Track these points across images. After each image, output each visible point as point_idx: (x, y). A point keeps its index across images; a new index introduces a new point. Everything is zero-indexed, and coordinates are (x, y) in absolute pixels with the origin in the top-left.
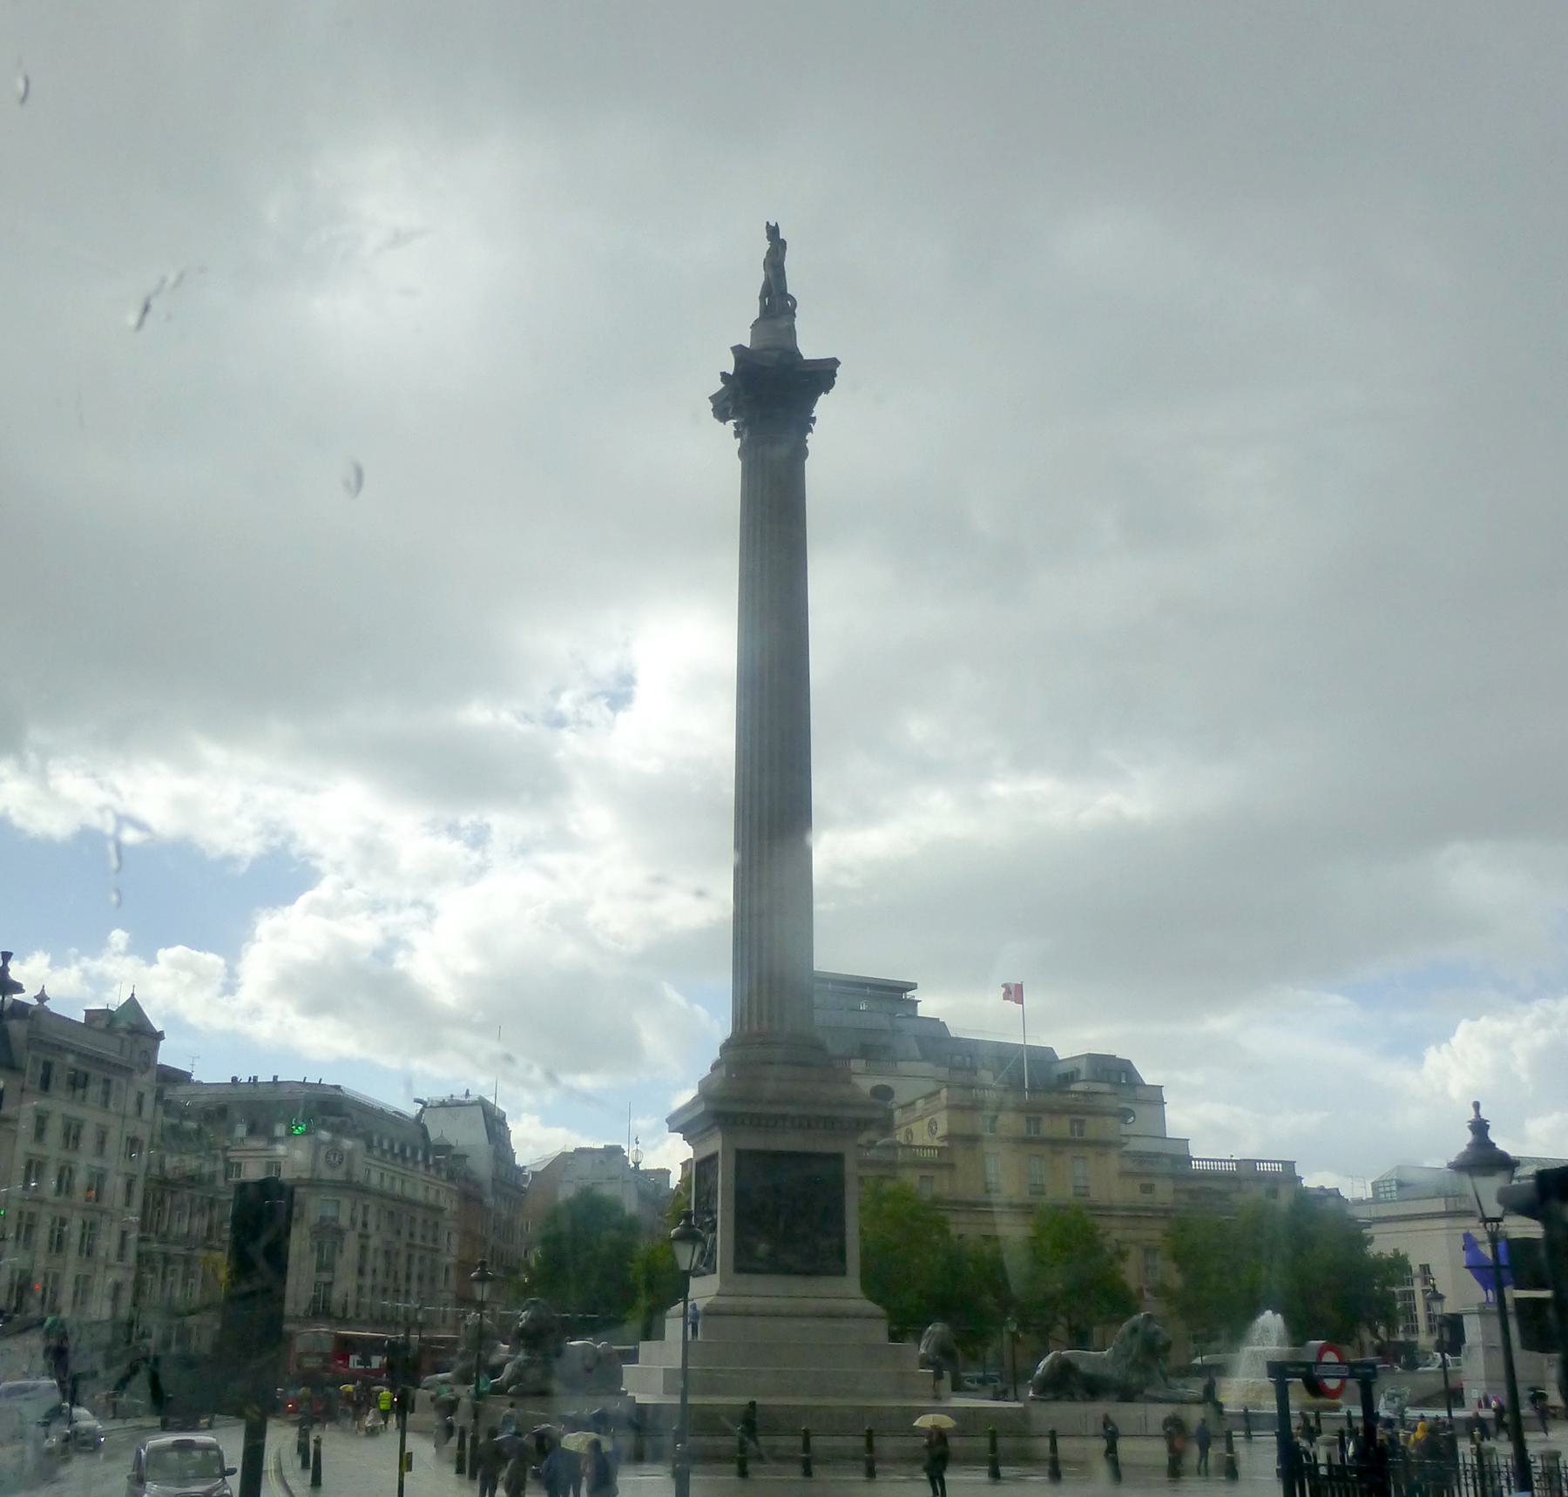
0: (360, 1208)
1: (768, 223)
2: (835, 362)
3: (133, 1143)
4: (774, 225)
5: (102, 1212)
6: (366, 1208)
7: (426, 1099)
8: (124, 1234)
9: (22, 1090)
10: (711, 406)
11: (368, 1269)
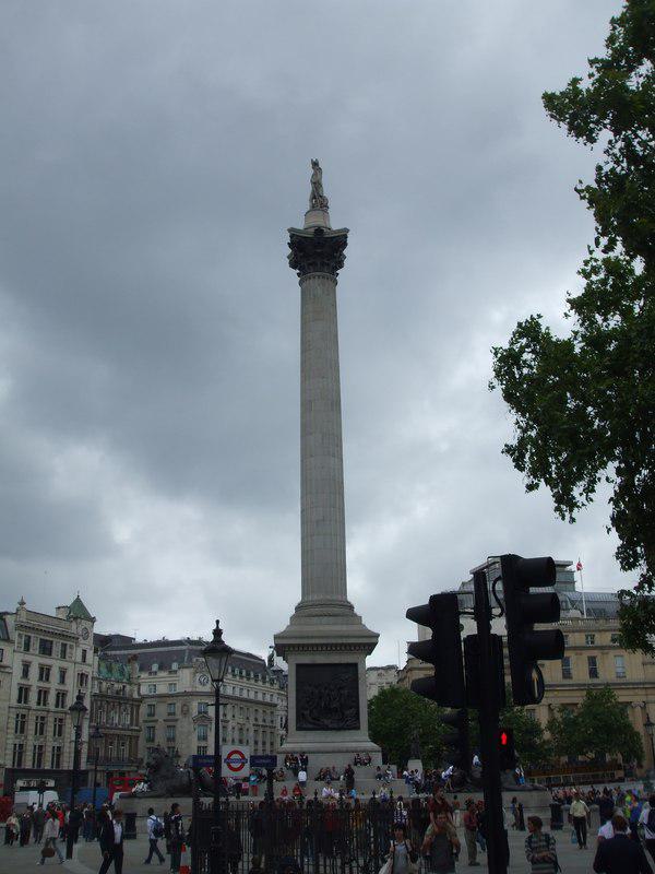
3: (82, 677)
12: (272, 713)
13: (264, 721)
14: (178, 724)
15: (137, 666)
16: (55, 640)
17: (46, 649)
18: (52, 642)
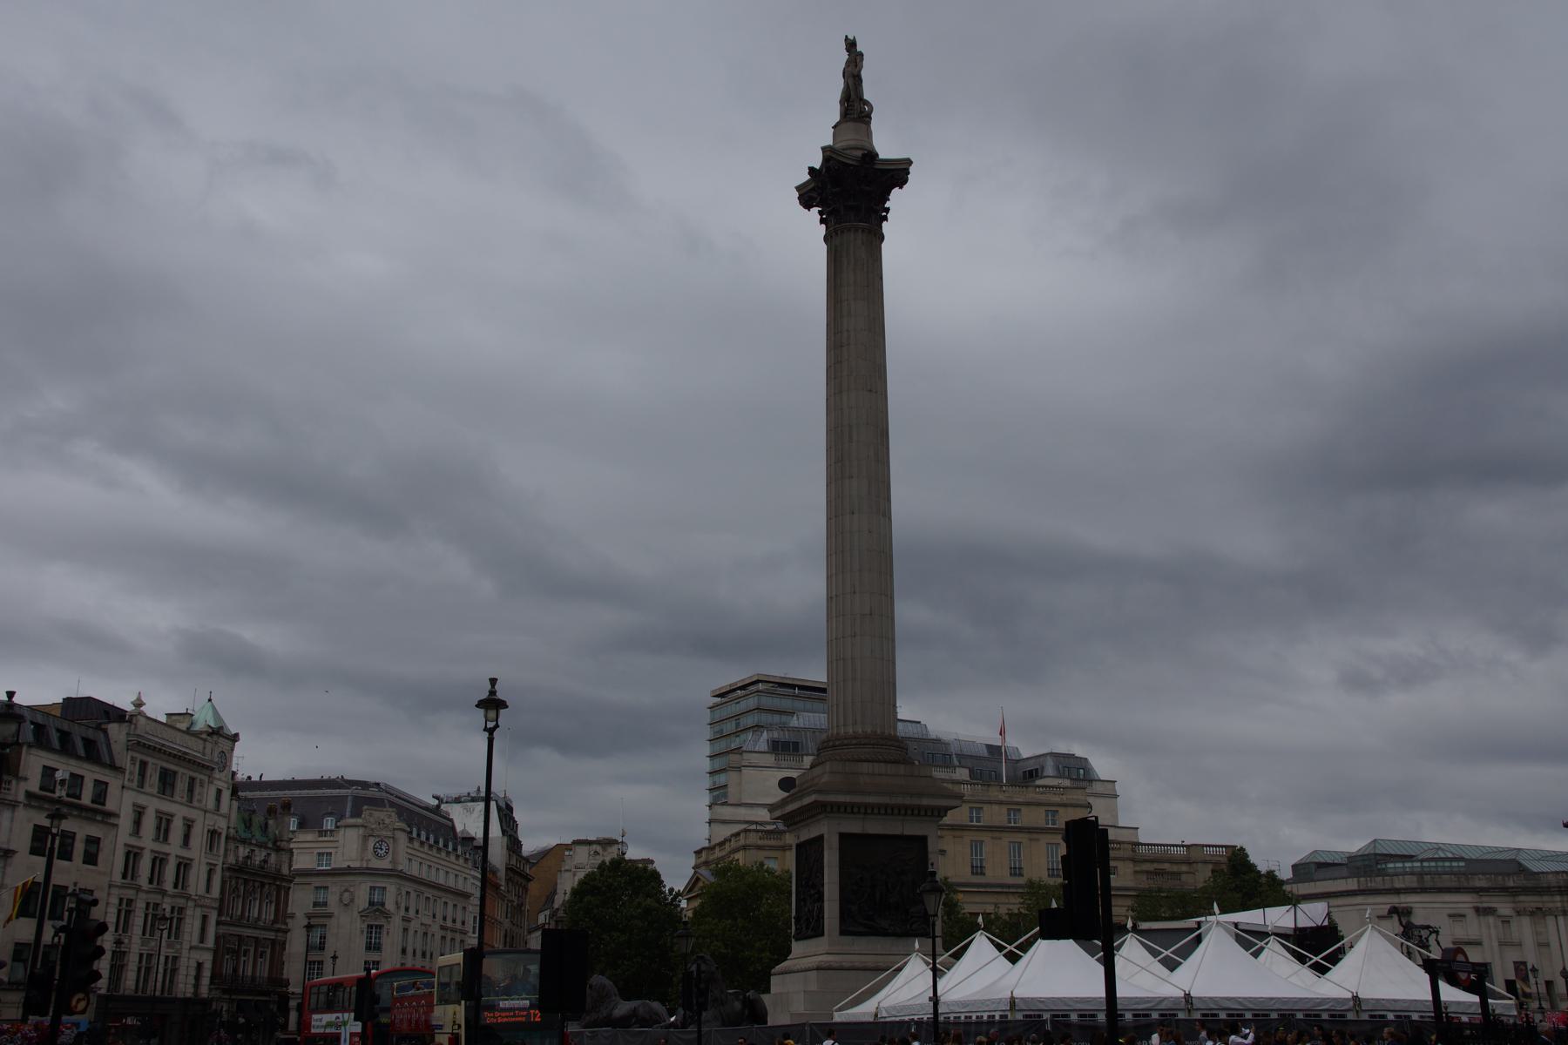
0: (404, 893)
1: (846, 36)
2: (909, 162)
3: (213, 834)
4: (852, 38)
5: (188, 898)
6: (408, 893)
7: (442, 796)
8: (205, 918)
9: (123, 787)
10: (797, 195)
11: (410, 950)
12: (464, 908)
13: (454, 921)
14: (332, 923)
15: (293, 823)
16: (181, 770)
17: (167, 782)
18: (175, 773)
